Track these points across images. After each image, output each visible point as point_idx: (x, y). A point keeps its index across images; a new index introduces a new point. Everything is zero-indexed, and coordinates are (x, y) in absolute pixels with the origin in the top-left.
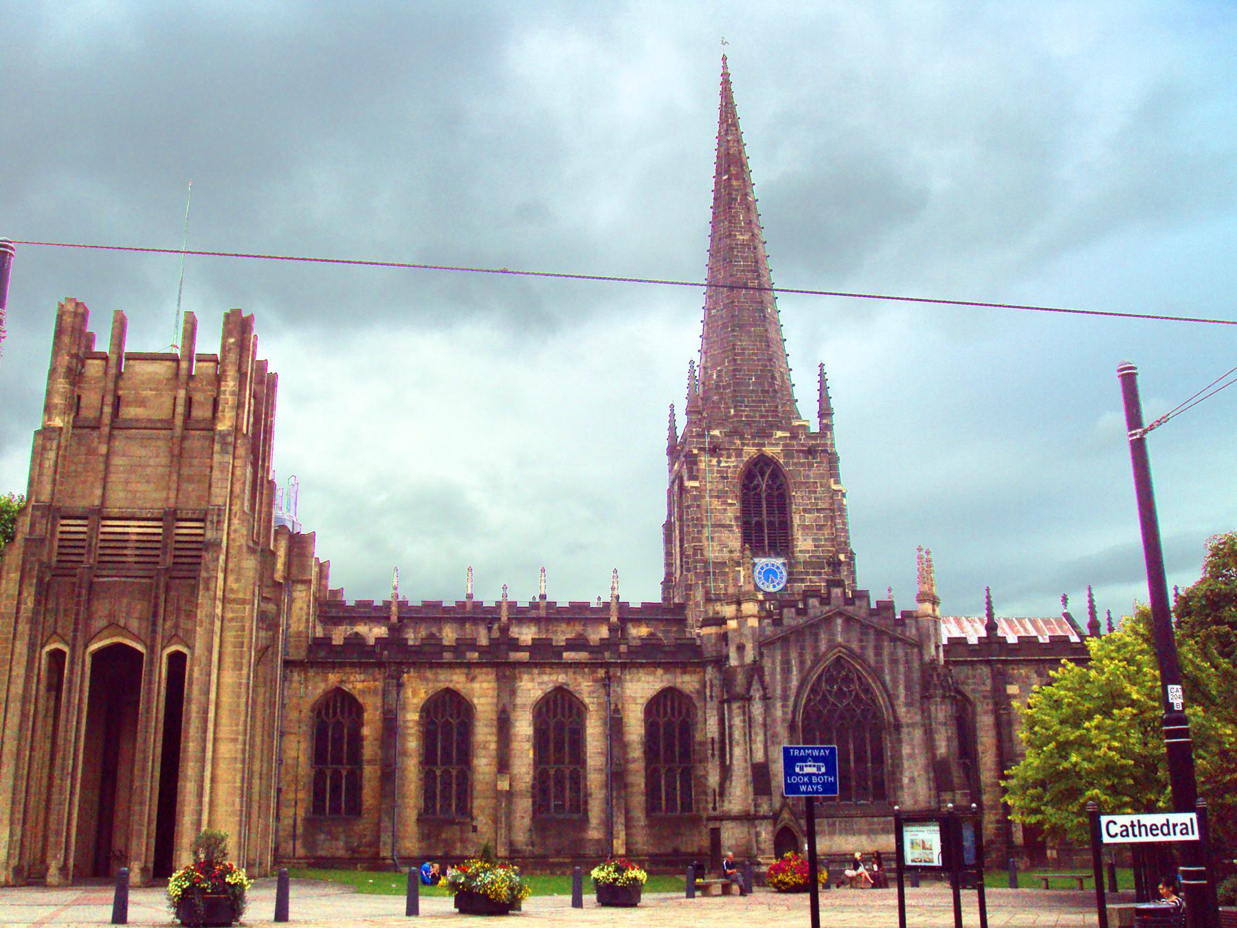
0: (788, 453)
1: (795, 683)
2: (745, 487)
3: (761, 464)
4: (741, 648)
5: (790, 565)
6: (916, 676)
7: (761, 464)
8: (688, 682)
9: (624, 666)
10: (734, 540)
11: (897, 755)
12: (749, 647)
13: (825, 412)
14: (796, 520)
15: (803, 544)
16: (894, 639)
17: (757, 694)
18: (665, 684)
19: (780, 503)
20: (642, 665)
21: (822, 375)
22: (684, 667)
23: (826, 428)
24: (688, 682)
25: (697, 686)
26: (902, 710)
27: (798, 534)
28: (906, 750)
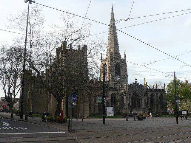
0: (121, 62)
1: (132, 93)
2: (116, 67)
3: (118, 63)
4: (126, 89)
5: (121, 77)
6: (144, 93)
7: (118, 63)
8: (116, 92)
9: (109, 90)
10: (115, 74)
11: (141, 103)
12: (128, 89)
13: (125, 57)
14: (122, 71)
15: (122, 75)
16: (141, 89)
17: (129, 95)
18: (112, 93)
19: (119, 68)
20: (110, 90)
21: (125, 52)
22: (115, 90)
23: (125, 59)
24: (116, 92)
25: (116, 93)
26: (142, 97)
27: (122, 73)
28: (142, 102)
